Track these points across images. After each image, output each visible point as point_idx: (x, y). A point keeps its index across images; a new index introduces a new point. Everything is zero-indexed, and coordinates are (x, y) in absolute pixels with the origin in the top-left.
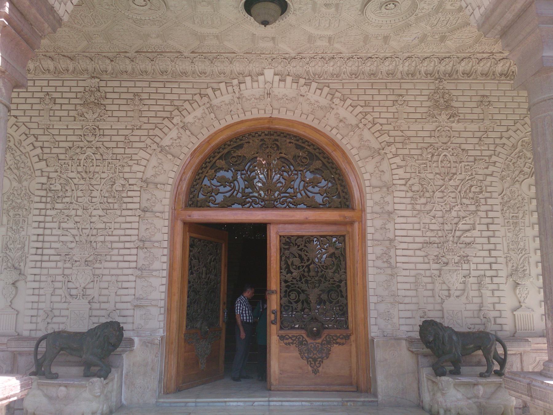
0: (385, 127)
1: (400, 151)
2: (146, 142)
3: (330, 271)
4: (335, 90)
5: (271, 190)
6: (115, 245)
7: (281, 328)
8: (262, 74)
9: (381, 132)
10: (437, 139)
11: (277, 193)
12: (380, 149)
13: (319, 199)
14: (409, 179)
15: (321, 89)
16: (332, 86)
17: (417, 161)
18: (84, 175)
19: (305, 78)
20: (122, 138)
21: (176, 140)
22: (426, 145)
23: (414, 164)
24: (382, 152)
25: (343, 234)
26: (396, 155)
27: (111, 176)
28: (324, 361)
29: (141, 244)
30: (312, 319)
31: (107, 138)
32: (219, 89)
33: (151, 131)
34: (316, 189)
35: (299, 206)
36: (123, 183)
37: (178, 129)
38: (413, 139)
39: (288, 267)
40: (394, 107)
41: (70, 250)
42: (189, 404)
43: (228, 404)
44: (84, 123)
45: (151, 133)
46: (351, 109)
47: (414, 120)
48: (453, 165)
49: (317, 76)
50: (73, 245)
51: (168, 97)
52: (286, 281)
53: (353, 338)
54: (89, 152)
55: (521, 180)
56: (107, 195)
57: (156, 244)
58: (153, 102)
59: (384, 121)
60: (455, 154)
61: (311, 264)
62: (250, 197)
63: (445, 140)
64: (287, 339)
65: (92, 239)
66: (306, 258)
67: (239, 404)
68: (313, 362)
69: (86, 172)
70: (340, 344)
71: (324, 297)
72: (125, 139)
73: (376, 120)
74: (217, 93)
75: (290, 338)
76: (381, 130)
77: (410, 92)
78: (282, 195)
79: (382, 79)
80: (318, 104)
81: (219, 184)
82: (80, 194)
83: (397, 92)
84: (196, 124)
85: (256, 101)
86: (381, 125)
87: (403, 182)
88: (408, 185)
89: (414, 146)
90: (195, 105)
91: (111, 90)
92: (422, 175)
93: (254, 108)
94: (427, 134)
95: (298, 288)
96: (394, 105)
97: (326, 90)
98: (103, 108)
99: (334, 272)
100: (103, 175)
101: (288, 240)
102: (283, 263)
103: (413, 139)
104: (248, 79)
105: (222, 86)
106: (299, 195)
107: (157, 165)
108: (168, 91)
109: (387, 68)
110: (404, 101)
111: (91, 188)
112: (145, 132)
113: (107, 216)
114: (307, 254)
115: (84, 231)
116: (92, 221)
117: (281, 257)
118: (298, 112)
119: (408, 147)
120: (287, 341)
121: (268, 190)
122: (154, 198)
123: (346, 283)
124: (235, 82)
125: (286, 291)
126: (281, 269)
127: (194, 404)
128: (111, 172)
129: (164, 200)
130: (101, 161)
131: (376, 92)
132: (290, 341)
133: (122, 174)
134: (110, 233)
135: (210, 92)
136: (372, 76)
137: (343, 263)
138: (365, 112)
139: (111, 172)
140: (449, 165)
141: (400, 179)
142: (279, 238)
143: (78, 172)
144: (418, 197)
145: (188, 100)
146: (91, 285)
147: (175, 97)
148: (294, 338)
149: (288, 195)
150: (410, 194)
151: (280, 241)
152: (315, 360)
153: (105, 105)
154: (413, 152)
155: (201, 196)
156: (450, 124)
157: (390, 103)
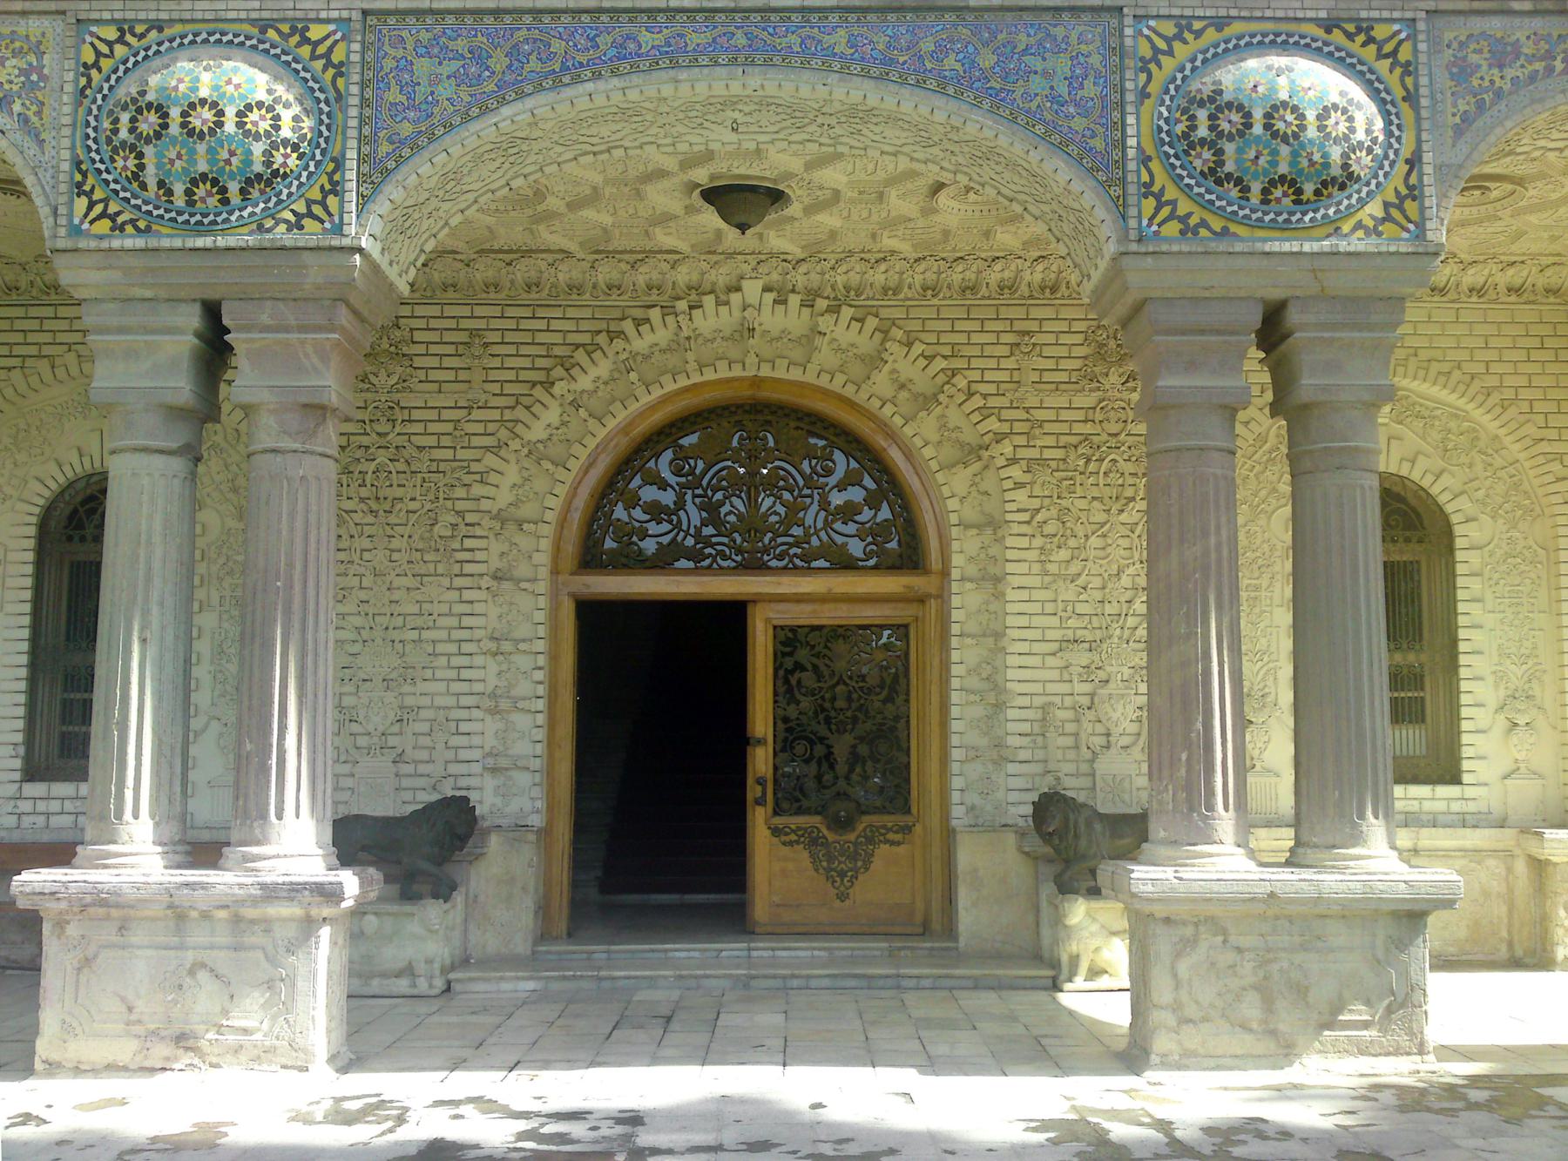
0: (992, 402)
1: (1022, 453)
2: (499, 435)
3: (874, 698)
4: (889, 323)
5: (756, 531)
6: (440, 648)
7: (776, 813)
8: (738, 289)
9: (985, 412)
10: (1098, 426)
11: (770, 535)
12: (981, 447)
13: (856, 548)
14: (1038, 511)
15: (861, 320)
16: (884, 313)
17: (1055, 474)
18: (374, 506)
19: (828, 298)
20: (449, 427)
21: (557, 429)
22: (1074, 440)
23: (1048, 479)
24: (985, 454)
25: (905, 622)
26: (1013, 461)
27: (428, 506)
28: (861, 877)
29: (493, 646)
30: (838, 794)
31: (419, 428)
32: (648, 320)
33: (507, 412)
34: (851, 528)
35: (815, 564)
36: (454, 522)
37: (561, 405)
38: (1048, 428)
39: (790, 690)
40: (1013, 358)
41: (351, 659)
42: (596, 956)
43: (671, 954)
44: (369, 395)
45: (508, 415)
46: (922, 362)
47: (1053, 386)
48: (1131, 480)
49: (852, 293)
50: (356, 648)
51: (541, 338)
52: (786, 720)
53: (918, 829)
54: (382, 457)
55: (1270, 509)
56: (420, 546)
57: (522, 646)
58: (512, 350)
59: (992, 389)
60: (1134, 459)
61: (838, 683)
62: (712, 545)
63: (1114, 428)
64: (787, 834)
65: (396, 635)
66: (826, 672)
67: (692, 954)
68: (838, 879)
69: (378, 498)
70: (892, 843)
71: (863, 750)
72: (455, 429)
73: (974, 387)
74: (645, 328)
75: (793, 831)
76: (984, 407)
77: (1047, 326)
78: (780, 540)
79: (989, 298)
80: (855, 351)
81: (648, 517)
82: (366, 544)
83: (1018, 326)
84: (600, 394)
85: (725, 344)
86: (985, 396)
87: (1025, 517)
88: (1034, 523)
89: (1050, 441)
90: (597, 355)
91: (421, 324)
92: (1064, 503)
93: (721, 359)
94: (1080, 415)
95: (812, 732)
96: (1012, 354)
97: (872, 323)
98: (407, 363)
99: (884, 702)
100: (413, 506)
101: (790, 635)
102: (780, 683)
103: (1048, 428)
104: (709, 301)
105: (655, 314)
106: (815, 541)
107: (519, 481)
108: (542, 325)
109: (999, 276)
110: (1034, 345)
111: (390, 532)
112: (496, 414)
113: (423, 589)
114: (828, 662)
115: (376, 618)
116: (393, 598)
117: (776, 670)
118: (813, 368)
119: (1039, 443)
120: (787, 839)
121: (749, 531)
122: (515, 551)
123: (908, 722)
124: (682, 305)
125: (785, 740)
126: (776, 694)
127: (605, 955)
128: (428, 498)
129: (536, 555)
130: (408, 475)
131: (976, 326)
132: (793, 837)
133: (450, 503)
134: (431, 624)
135: (628, 326)
136: (968, 292)
137: (902, 681)
138: (953, 370)
139: (428, 498)
140: (1120, 481)
141: (1019, 511)
142: (771, 631)
143: (362, 500)
144: (1054, 547)
145: (584, 345)
146: (396, 728)
147: (557, 338)
148: (800, 833)
149: (791, 540)
150: (1038, 542)
151: (775, 637)
152: (842, 874)
153: (410, 357)
154: (1048, 454)
155: (609, 544)
156: (1125, 395)
157: (1005, 350)
